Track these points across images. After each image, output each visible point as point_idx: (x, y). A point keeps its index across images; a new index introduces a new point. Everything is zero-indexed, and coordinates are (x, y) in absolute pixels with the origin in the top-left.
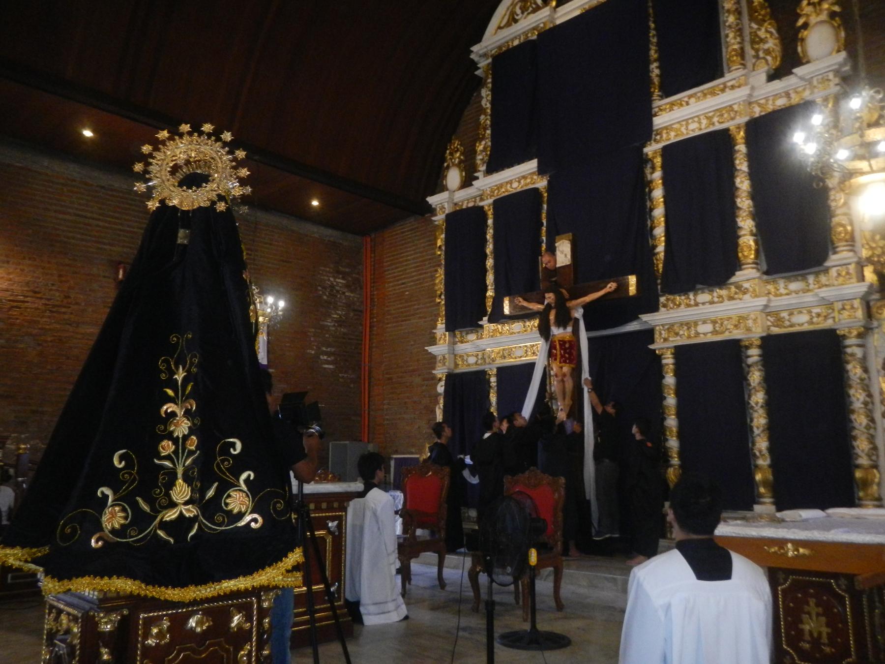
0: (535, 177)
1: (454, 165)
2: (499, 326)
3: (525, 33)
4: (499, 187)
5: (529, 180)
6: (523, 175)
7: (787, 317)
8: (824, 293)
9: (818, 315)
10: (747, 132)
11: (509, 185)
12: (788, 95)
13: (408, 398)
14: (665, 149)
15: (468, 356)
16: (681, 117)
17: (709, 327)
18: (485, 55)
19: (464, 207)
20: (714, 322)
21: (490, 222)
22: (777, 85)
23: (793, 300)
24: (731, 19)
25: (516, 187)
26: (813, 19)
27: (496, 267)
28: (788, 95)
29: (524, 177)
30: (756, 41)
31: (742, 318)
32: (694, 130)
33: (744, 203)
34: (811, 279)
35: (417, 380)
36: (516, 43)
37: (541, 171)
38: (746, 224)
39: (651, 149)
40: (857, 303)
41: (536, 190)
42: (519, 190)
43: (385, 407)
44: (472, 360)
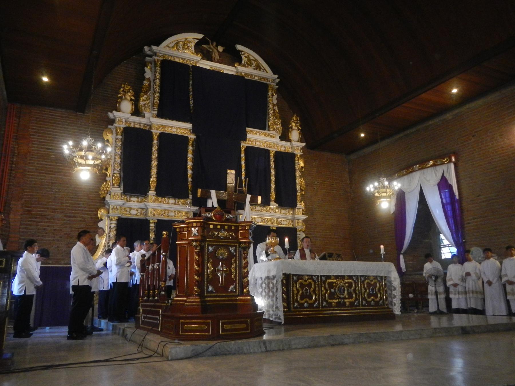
0: (186, 131)
1: (126, 99)
2: (160, 198)
3: (184, 59)
4: (164, 126)
5: (182, 131)
6: (181, 128)
8: (296, 216)
9: (288, 223)
10: (274, 155)
11: (170, 129)
12: (285, 147)
13: (48, 226)
14: (247, 147)
15: (130, 209)
16: (255, 138)
17: (260, 220)
18: (156, 54)
19: (132, 125)
20: (263, 218)
21: (155, 142)
22: (284, 143)
23: (284, 216)
24: (272, 112)
25: (174, 131)
26: (294, 128)
27: (159, 166)
28: (285, 147)
29: (180, 128)
30: (275, 124)
31: (270, 219)
32: (258, 145)
33: (273, 178)
34: (288, 210)
35: (60, 216)
36: (177, 60)
37: (194, 131)
38: (273, 186)
39: (244, 145)
40: (301, 221)
41: (187, 137)
42: (175, 133)
43: (21, 230)
44: (134, 212)
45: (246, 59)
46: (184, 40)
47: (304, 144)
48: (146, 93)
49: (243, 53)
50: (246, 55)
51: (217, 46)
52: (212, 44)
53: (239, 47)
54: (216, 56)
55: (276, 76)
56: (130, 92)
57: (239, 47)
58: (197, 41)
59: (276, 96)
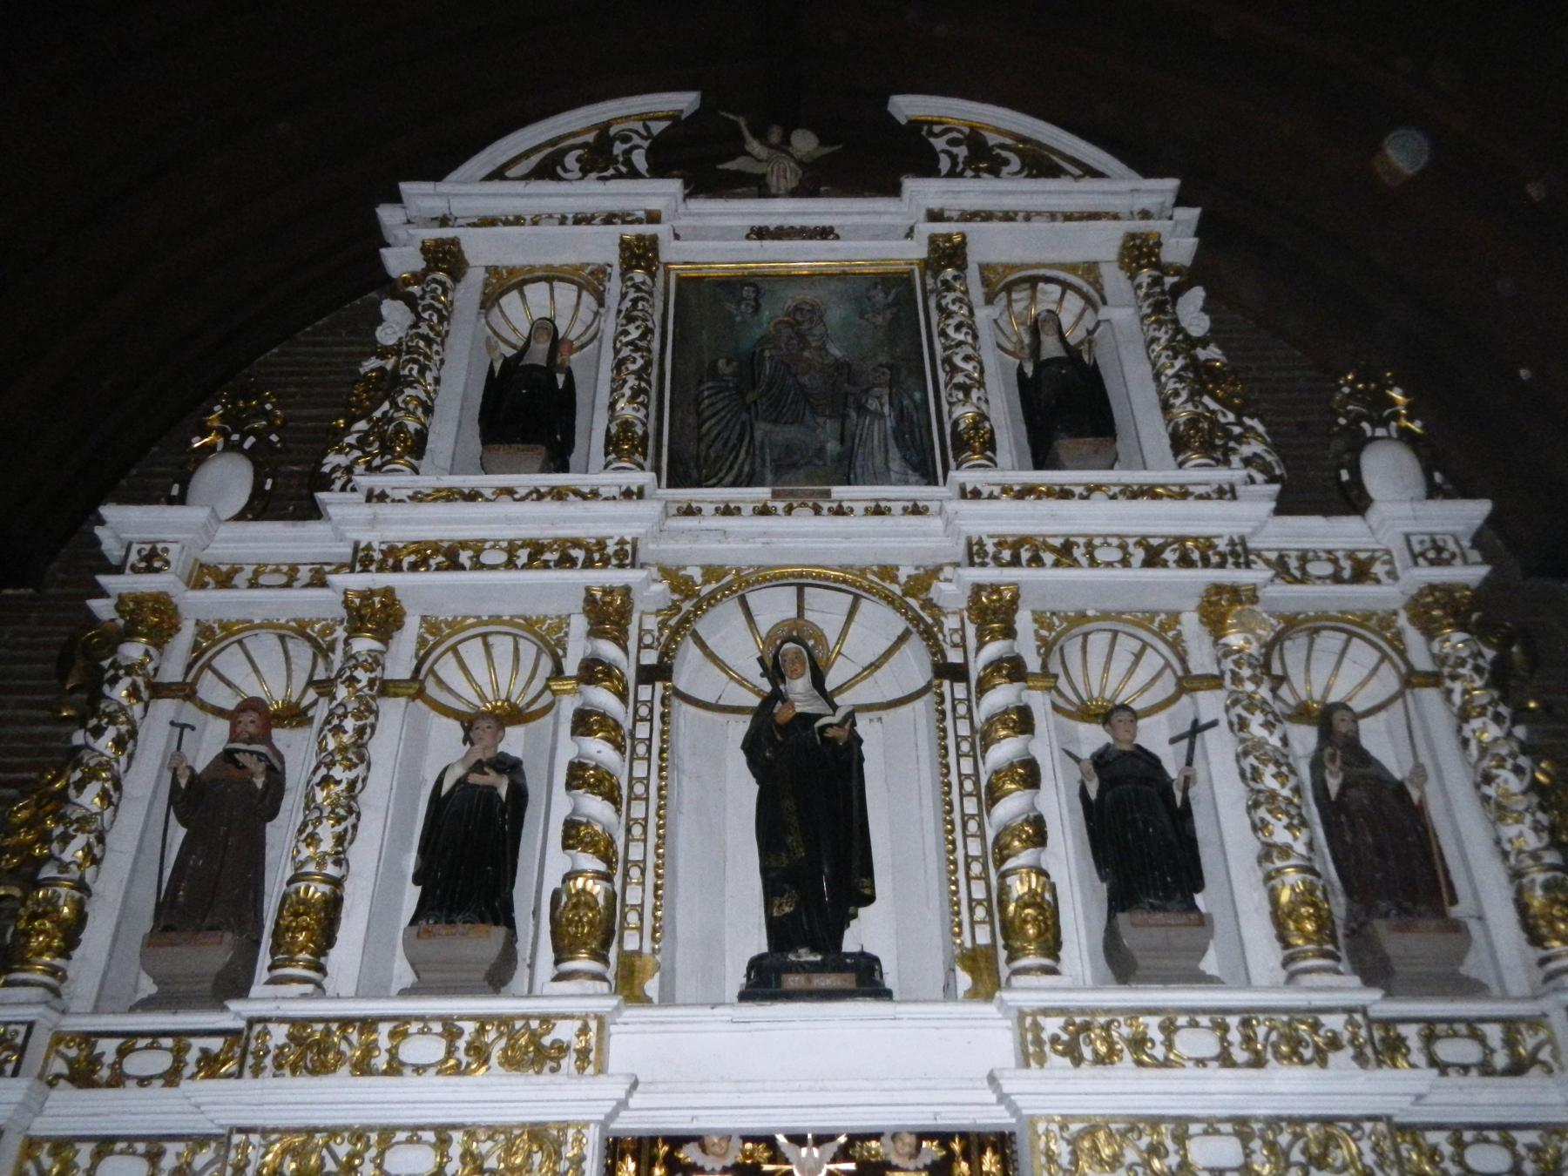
1: (231, 447)
7: (1447, 1149)
45: (962, 152)
46: (590, 138)
47: (1477, 510)
48: (366, 415)
49: (937, 129)
50: (955, 135)
51: (786, 141)
52: (760, 134)
53: (906, 107)
54: (784, 173)
55: (1172, 184)
56: (261, 413)
57: (906, 107)
58: (657, 127)
59: (1197, 295)
